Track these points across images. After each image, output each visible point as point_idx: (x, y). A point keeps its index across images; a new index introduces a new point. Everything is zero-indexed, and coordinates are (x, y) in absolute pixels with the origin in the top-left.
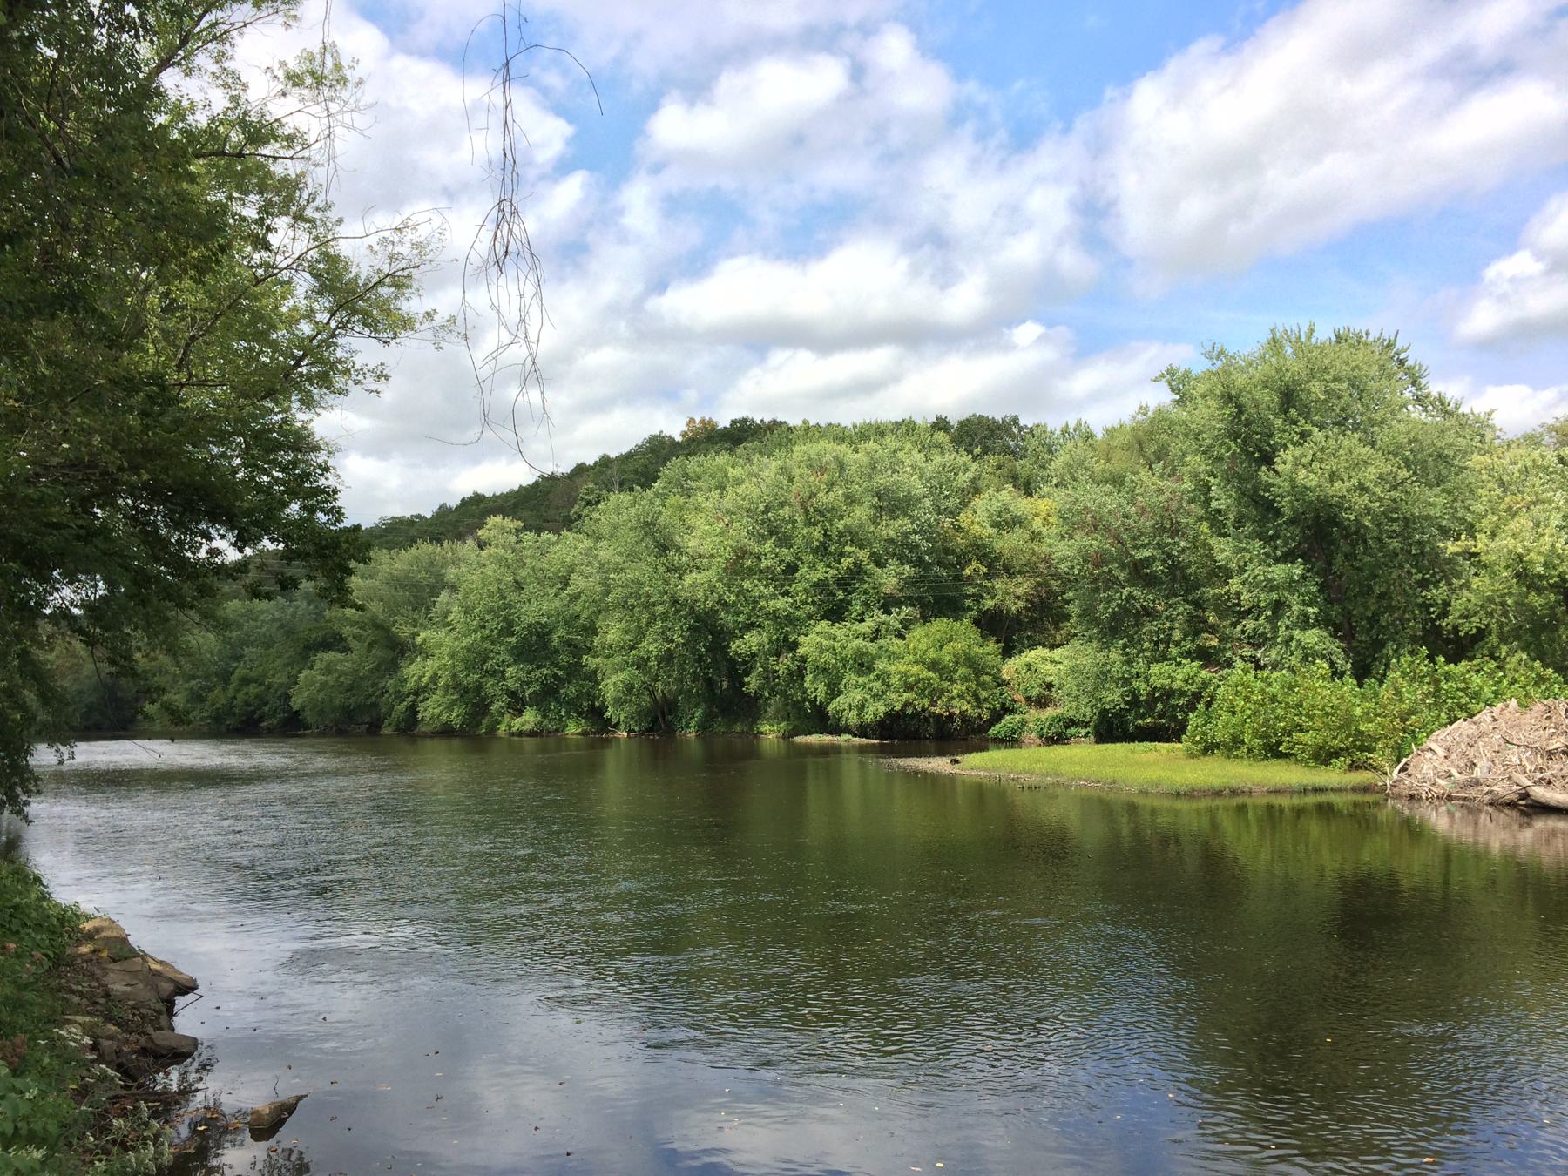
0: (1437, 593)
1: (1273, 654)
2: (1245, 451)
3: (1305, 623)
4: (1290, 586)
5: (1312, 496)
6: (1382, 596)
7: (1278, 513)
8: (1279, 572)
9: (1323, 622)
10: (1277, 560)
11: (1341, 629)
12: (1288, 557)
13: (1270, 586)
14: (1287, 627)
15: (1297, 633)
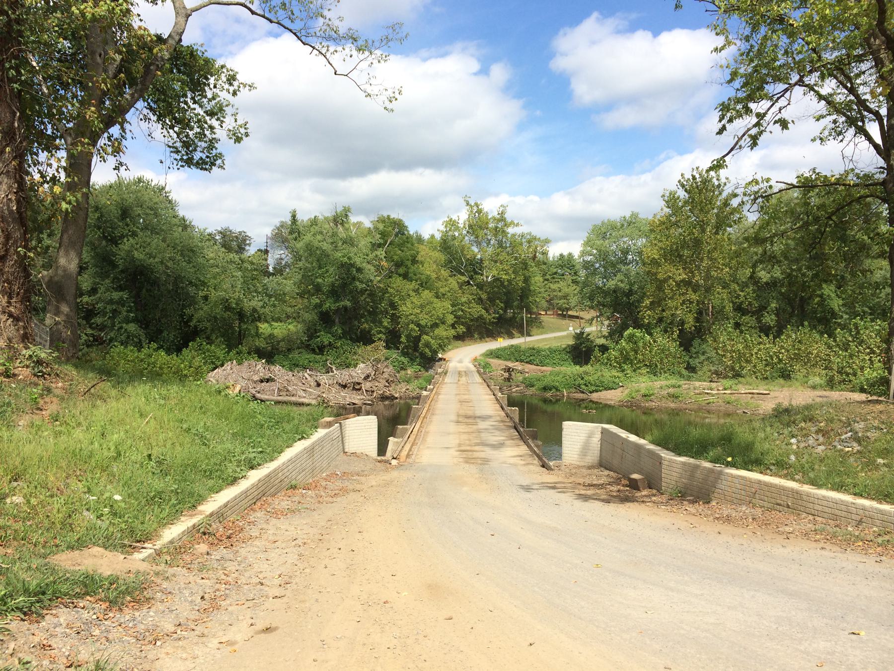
0: (188, 311)
1: (112, 334)
2: (104, 235)
3: (128, 321)
4: (121, 302)
5: (138, 263)
6: (162, 310)
7: (117, 266)
8: (116, 295)
9: (135, 320)
10: (116, 290)
11: (144, 323)
12: (120, 288)
13: (111, 302)
14: (119, 323)
15: (124, 325)
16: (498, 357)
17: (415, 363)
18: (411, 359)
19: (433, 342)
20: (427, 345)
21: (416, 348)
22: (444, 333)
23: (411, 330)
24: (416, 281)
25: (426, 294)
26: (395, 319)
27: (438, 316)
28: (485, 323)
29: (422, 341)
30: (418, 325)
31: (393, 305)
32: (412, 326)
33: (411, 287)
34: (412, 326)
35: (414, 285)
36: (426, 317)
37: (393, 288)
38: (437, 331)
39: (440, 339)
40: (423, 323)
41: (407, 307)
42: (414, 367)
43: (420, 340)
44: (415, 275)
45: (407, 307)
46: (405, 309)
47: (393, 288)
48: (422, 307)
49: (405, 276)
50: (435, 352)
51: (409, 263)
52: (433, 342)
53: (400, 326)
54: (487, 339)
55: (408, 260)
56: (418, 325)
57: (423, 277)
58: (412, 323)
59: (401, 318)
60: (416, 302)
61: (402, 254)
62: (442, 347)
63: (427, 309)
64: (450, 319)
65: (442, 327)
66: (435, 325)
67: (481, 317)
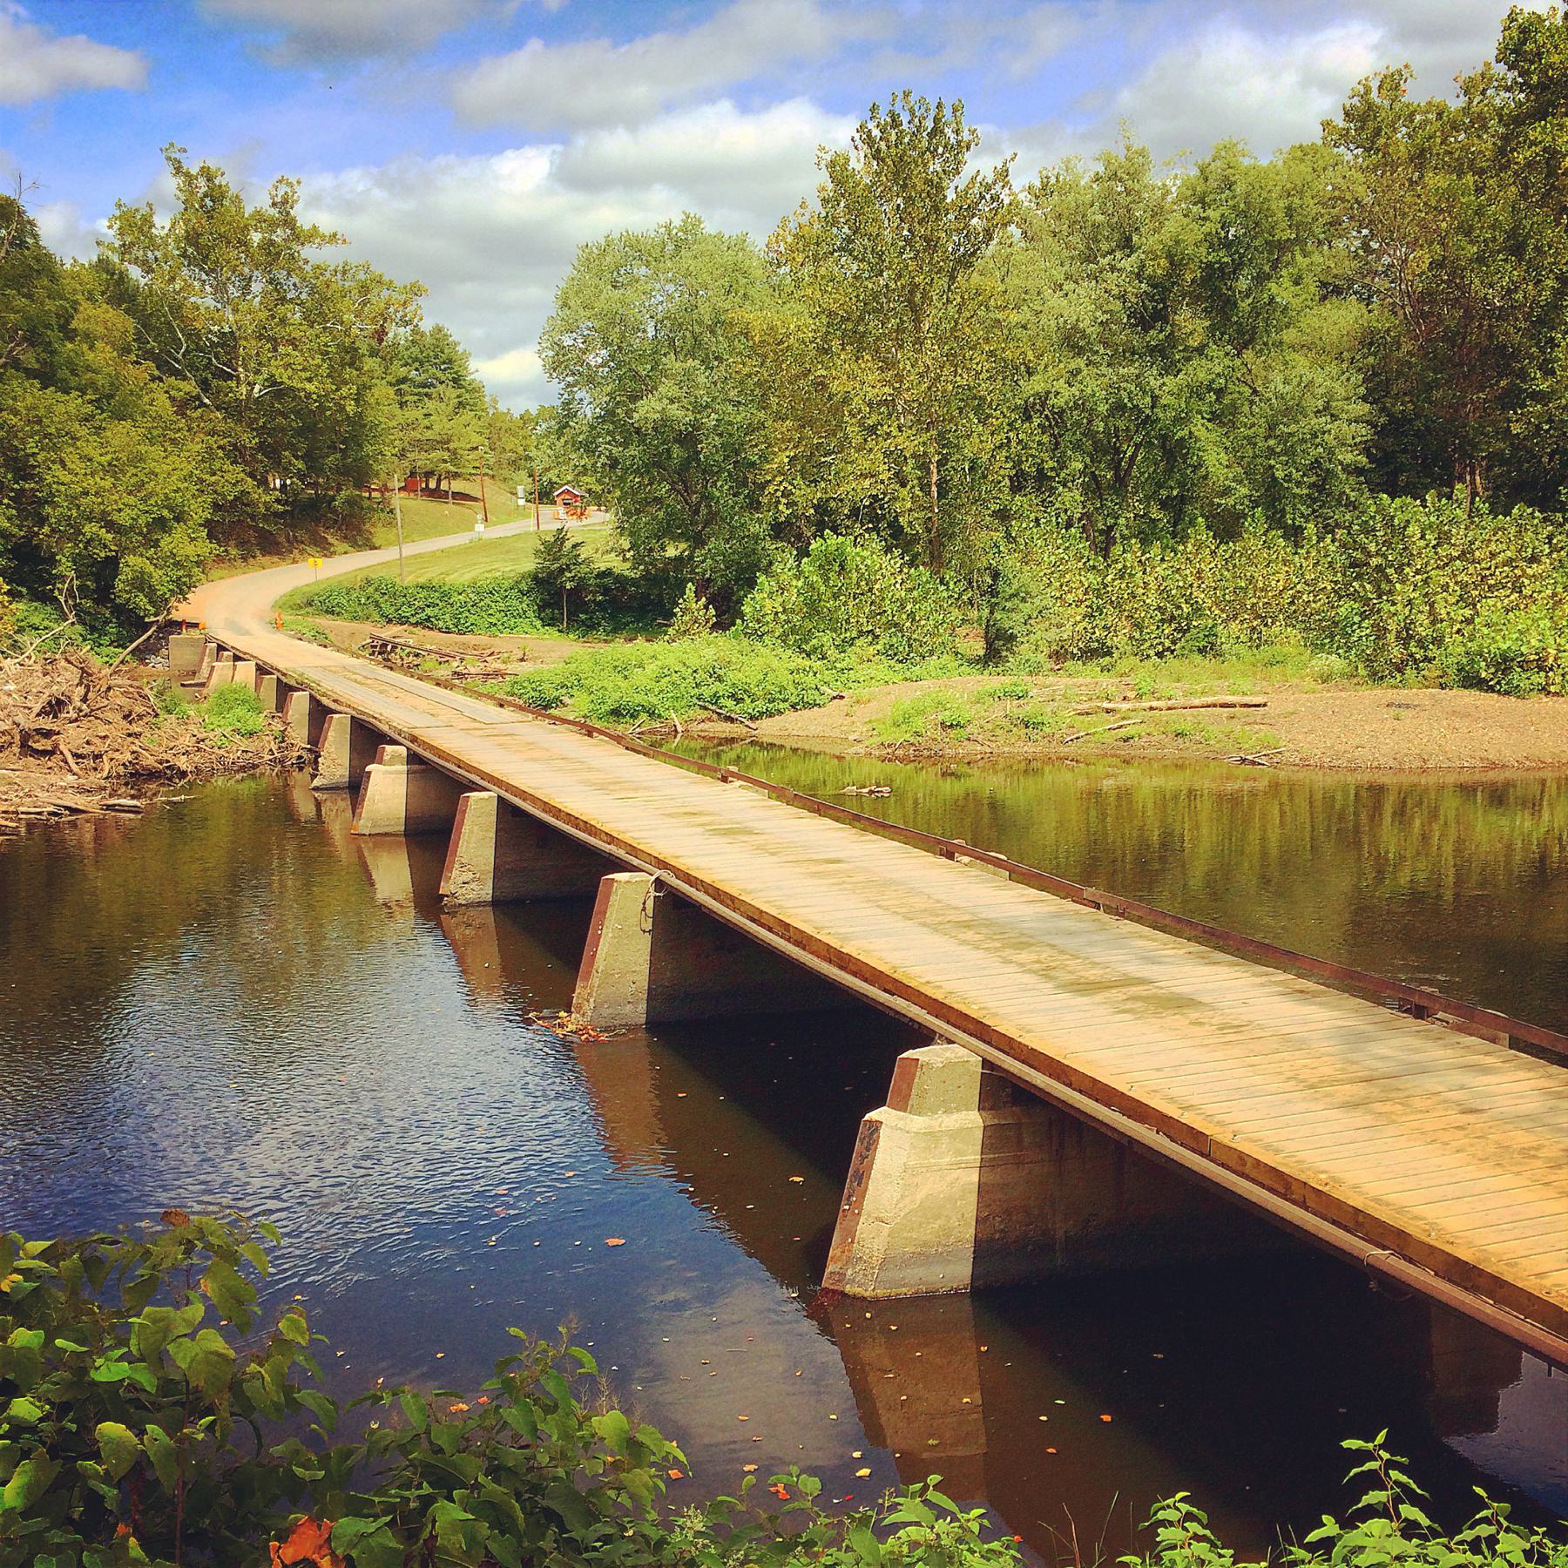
16: (332, 613)
17: (105, 640)
18: (93, 629)
19: (157, 574)
20: (141, 583)
21: (103, 593)
22: (190, 550)
23: (88, 542)
24: (83, 391)
25: (120, 434)
26: (31, 507)
27: (167, 498)
28: (253, 517)
29: (125, 574)
30: (110, 526)
31: (23, 469)
32: (90, 529)
33: (71, 407)
34: (90, 529)
35: (74, 403)
36: (131, 500)
37: (16, 413)
38: (166, 542)
39: (177, 564)
40: (124, 518)
41: (71, 472)
42: (104, 650)
43: (115, 572)
44: (73, 372)
45: (71, 472)
46: (66, 477)
47: (16, 413)
48: (112, 469)
49: (47, 377)
50: (160, 603)
51: (53, 335)
52: (157, 574)
53: (46, 530)
54: (266, 560)
55: (48, 326)
56: (110, 526)
57: (101, 380)
58: (90, 520)
59: (55, 505)
60: (95, 454)
61: (33, 309)
62: (182, 589)
63: (128, 479)
64: (199, 510)
65: (179, 531)
66: (161, 524)
67: (242, 499)
